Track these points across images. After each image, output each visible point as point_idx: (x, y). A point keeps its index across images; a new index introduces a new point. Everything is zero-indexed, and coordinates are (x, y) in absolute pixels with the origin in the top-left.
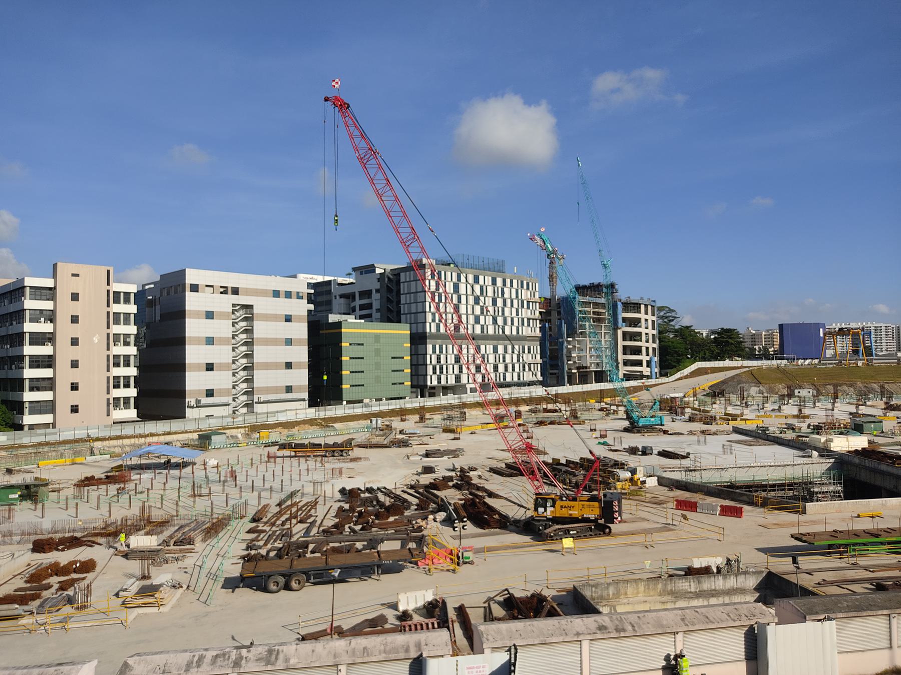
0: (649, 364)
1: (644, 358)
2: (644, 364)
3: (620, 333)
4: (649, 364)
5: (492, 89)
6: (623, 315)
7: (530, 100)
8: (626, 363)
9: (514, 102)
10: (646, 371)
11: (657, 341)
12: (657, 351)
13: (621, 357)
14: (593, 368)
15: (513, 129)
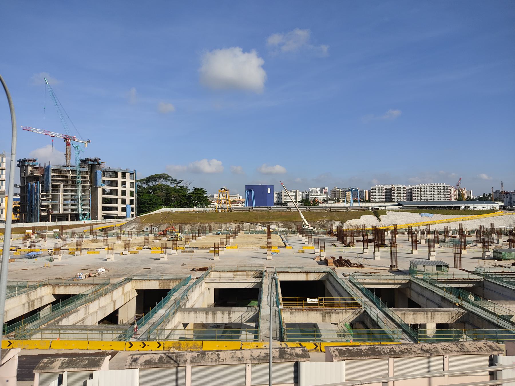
0: (124, 209)
1: (120, 206)
2: (120, 209)
3: (100, 190)
4: (124, 209)
5: (226, 43)
6: (100, 179)
7: (246, 50)
8: (105, 209)
9: (238, 51)
10: (120, 213)
11: (136, 195)
12: (135, 202)
13: (100, 205)
14: (69, 212)
15: (239, 67)
